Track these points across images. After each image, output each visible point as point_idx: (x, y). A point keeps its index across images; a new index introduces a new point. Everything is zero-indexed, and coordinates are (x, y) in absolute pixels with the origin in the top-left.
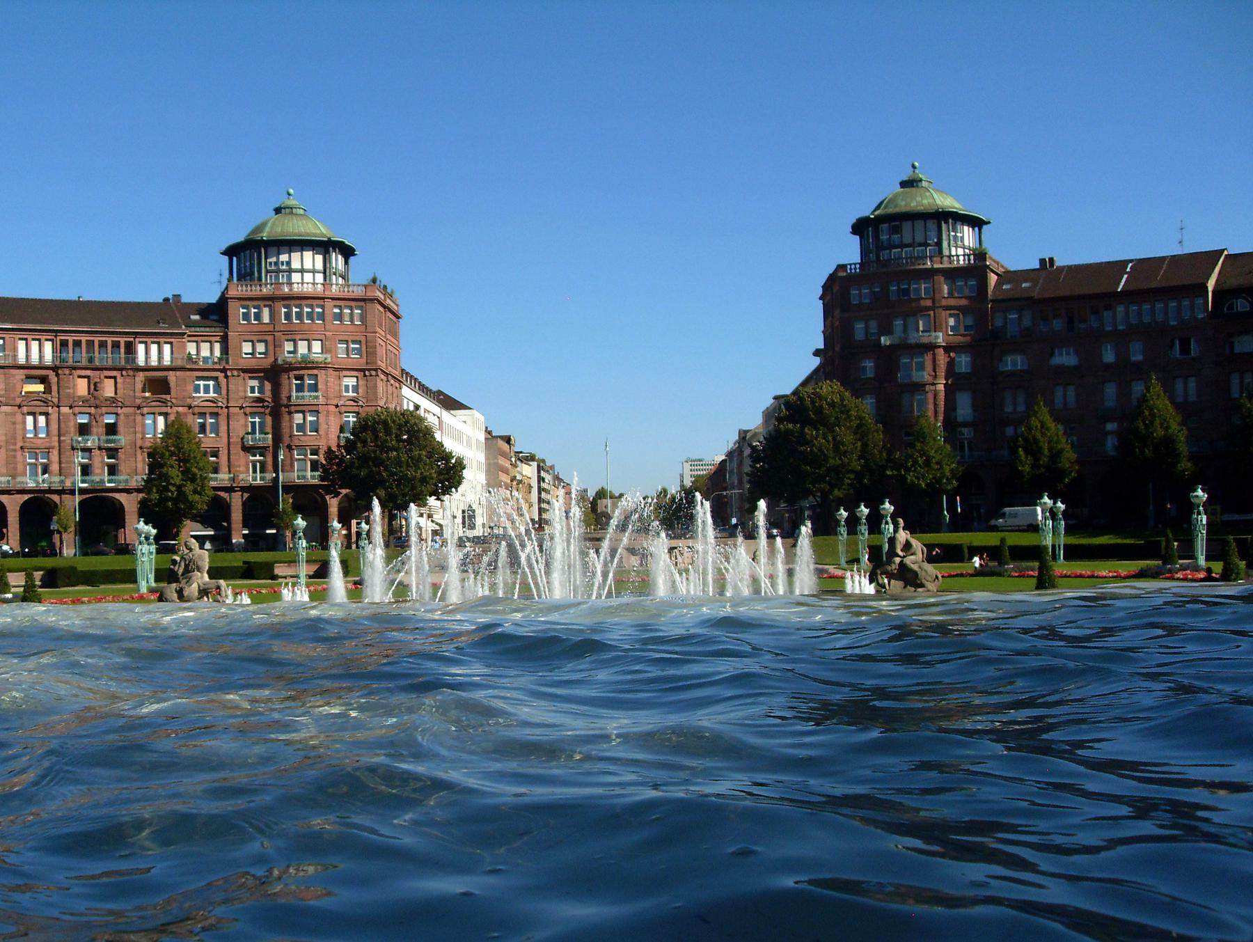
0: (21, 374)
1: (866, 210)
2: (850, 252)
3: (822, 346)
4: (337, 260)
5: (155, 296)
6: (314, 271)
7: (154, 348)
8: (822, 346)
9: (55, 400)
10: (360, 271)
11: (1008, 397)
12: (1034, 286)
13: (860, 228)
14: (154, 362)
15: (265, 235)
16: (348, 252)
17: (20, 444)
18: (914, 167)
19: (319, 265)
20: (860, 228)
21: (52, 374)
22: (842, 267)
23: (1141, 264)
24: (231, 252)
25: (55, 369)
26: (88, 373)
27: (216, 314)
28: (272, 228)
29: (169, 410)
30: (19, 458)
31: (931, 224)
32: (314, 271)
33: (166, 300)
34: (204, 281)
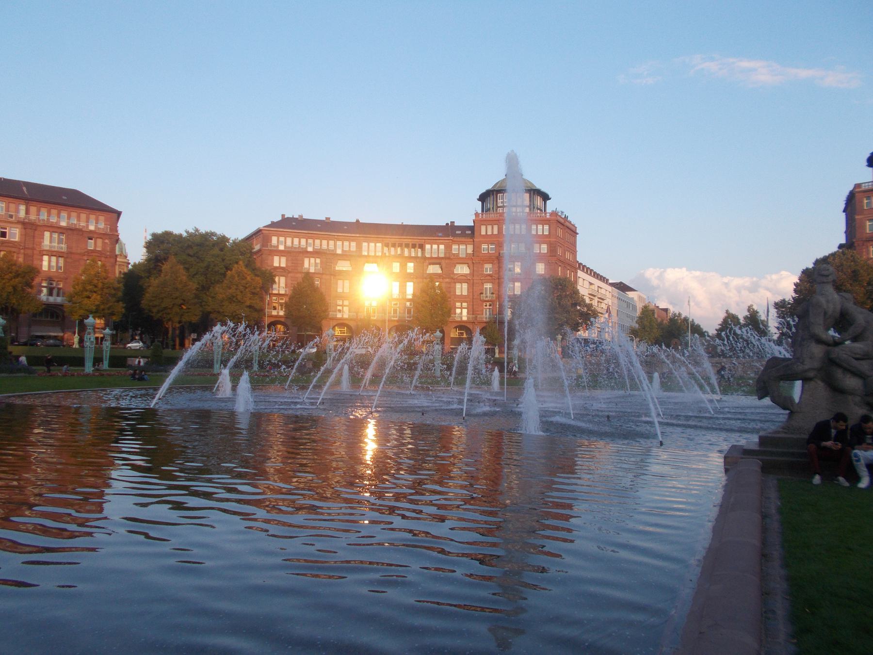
3: (843, 241)
4: (539, 201)
6: (523, 206)
8: (843, 241)
10: (551, 206)
19: (527, 202)
34: (465, 213)
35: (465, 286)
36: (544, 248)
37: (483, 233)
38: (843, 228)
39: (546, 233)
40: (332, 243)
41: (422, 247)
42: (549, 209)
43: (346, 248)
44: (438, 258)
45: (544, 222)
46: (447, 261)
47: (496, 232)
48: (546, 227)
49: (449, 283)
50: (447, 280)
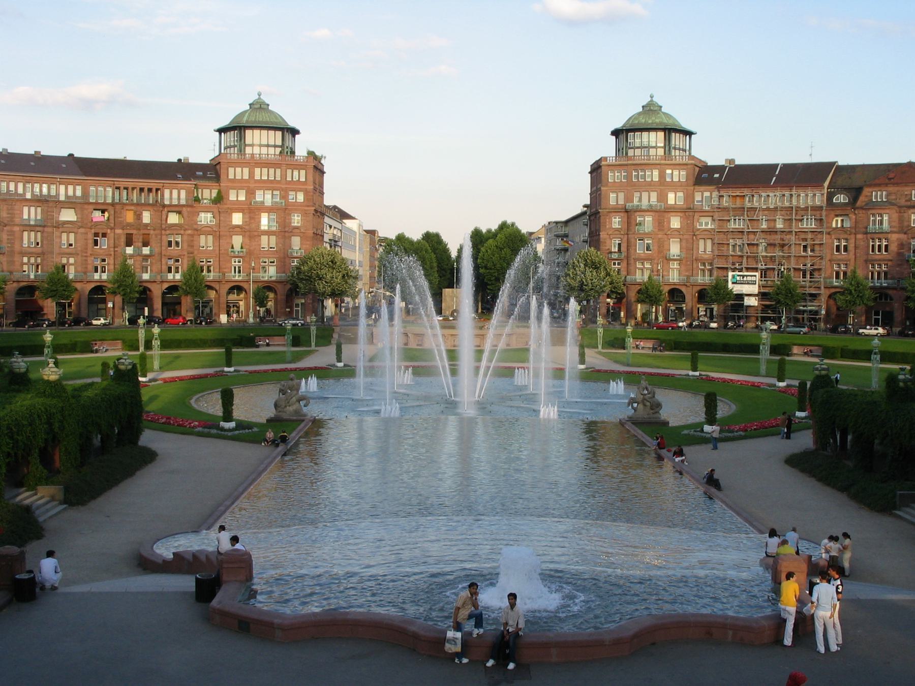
0: (92, 207)
1: (619, 125)
2: (608, 148)
5: (171, 157)
6: (275, 146)
7: (175, 192)
9: (112, 225)
11: (701, 242)
12: (721, 176)
13: (616, 133)
14: (175, 202)
15: (244, 121)
16: (294, 132)
17: (89, 252)
18: (652, 97)
19: (279, 142)
20: (616, 133)
21: (110, 208)
22: (606, 159)
23: (785, 166)
24: (221, 131)
25: (113, 204)
26: (133, 208)
27: (211, 172)
28: (249, 117)
29: (182, 232)
30: (90, 262)
31: (661, 135)
32: (275, 146)
33: (180, 160)
35: (210, 238)
36: (301, 197)
37: (231, 176)
38: (588, 190)
39: (303, 179)
40: (53, 187)
41: (157, 190)
42: (301, 152)
43: (71, 193)
44: (179, 206)
45: (299, 166)
46: (189, 209)
47: (246, 177)
48: (303, 172)
49: (192, 236)
50: (189, 232)
